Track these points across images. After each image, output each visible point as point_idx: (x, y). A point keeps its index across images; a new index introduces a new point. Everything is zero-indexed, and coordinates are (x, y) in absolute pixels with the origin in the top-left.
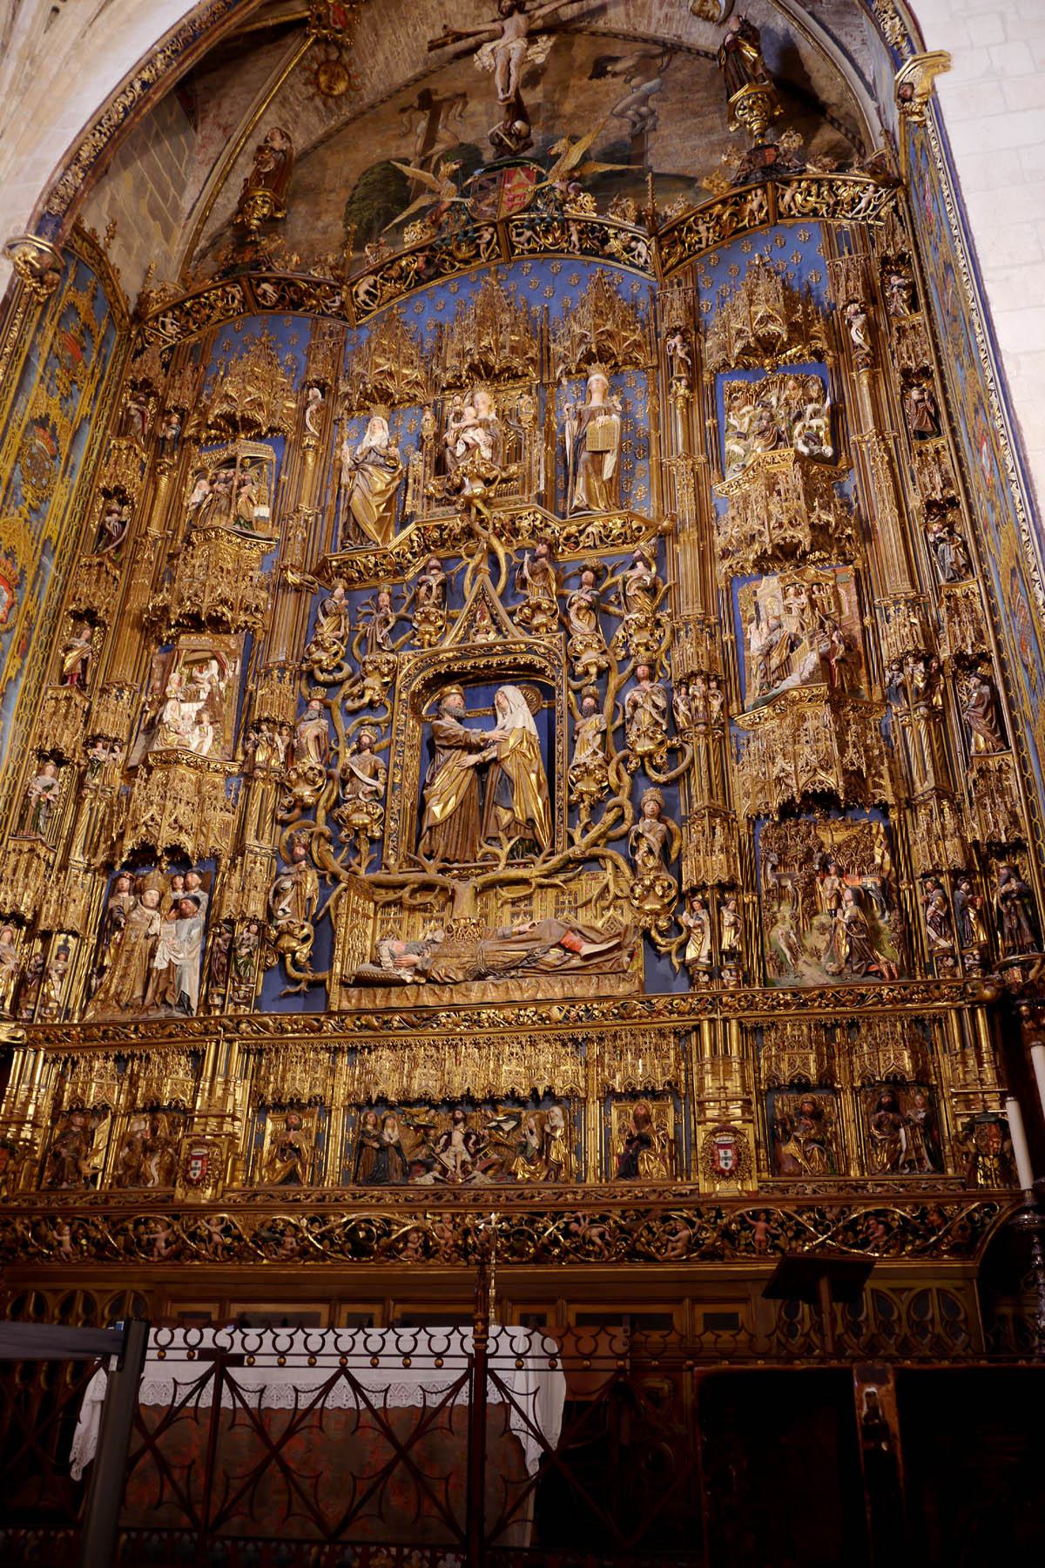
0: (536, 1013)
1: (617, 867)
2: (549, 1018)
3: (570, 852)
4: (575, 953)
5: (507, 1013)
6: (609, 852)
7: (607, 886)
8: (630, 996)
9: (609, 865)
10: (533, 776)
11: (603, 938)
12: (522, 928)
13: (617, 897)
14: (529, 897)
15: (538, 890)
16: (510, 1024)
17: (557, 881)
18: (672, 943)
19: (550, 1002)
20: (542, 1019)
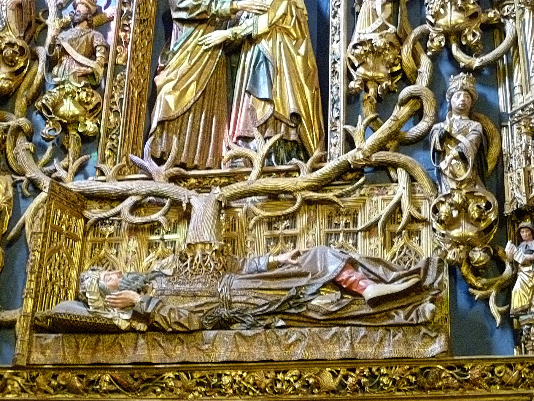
0: (300, 377)
1: (412, 179)
2: (317, 385)
3: (349, 157)
4: (358, 295)
5: (259, 376)
6: (402, 158)
7: (399, 204)
8: (435, 359)
9: (401, 175)
10: (299, 60)
11: (394, 275)
12: (281, 258)
13: (412, 219)
14: (292, 217)
15: (306, 207)
16: (263, 391)
17: (330, 195)
18: (489, 286)
19: (322, 362)
20: (307, 385)
